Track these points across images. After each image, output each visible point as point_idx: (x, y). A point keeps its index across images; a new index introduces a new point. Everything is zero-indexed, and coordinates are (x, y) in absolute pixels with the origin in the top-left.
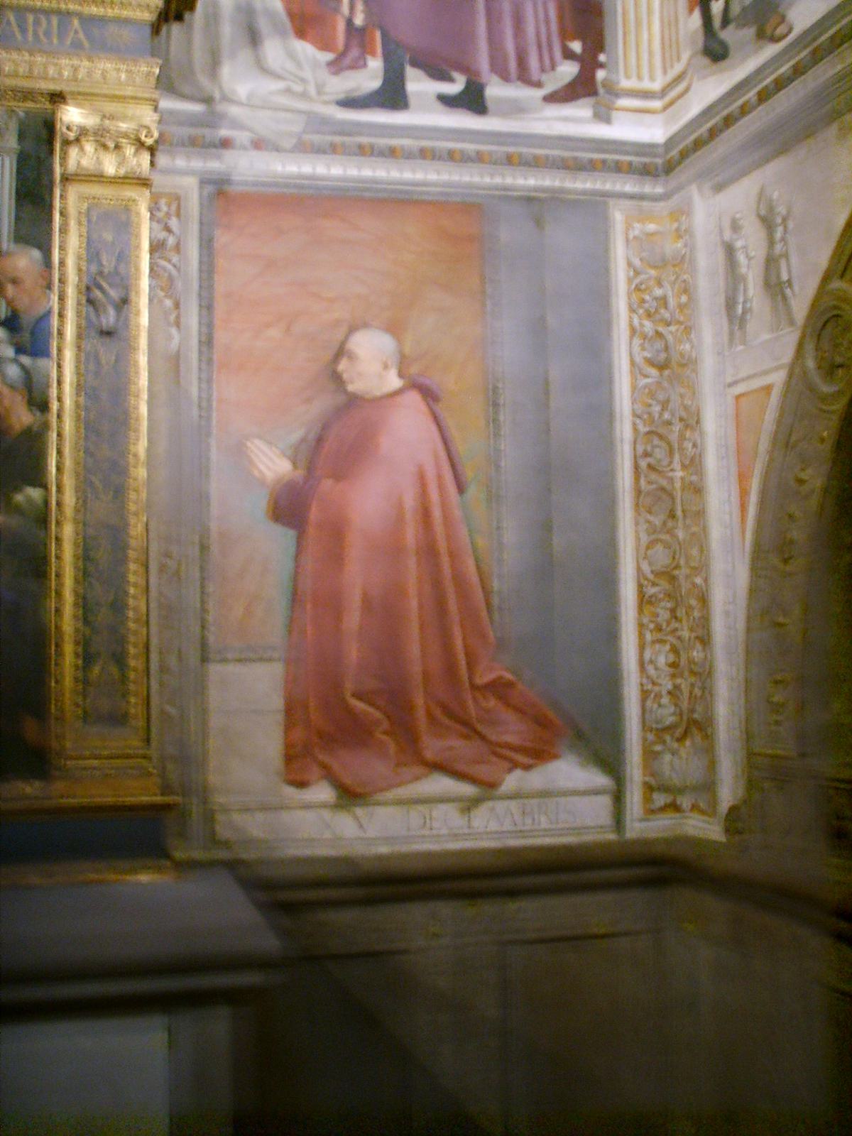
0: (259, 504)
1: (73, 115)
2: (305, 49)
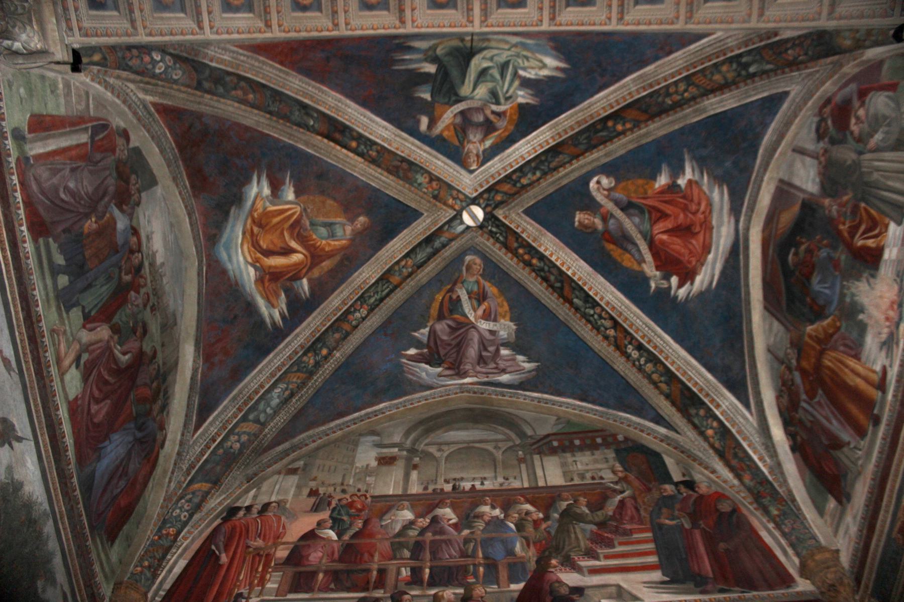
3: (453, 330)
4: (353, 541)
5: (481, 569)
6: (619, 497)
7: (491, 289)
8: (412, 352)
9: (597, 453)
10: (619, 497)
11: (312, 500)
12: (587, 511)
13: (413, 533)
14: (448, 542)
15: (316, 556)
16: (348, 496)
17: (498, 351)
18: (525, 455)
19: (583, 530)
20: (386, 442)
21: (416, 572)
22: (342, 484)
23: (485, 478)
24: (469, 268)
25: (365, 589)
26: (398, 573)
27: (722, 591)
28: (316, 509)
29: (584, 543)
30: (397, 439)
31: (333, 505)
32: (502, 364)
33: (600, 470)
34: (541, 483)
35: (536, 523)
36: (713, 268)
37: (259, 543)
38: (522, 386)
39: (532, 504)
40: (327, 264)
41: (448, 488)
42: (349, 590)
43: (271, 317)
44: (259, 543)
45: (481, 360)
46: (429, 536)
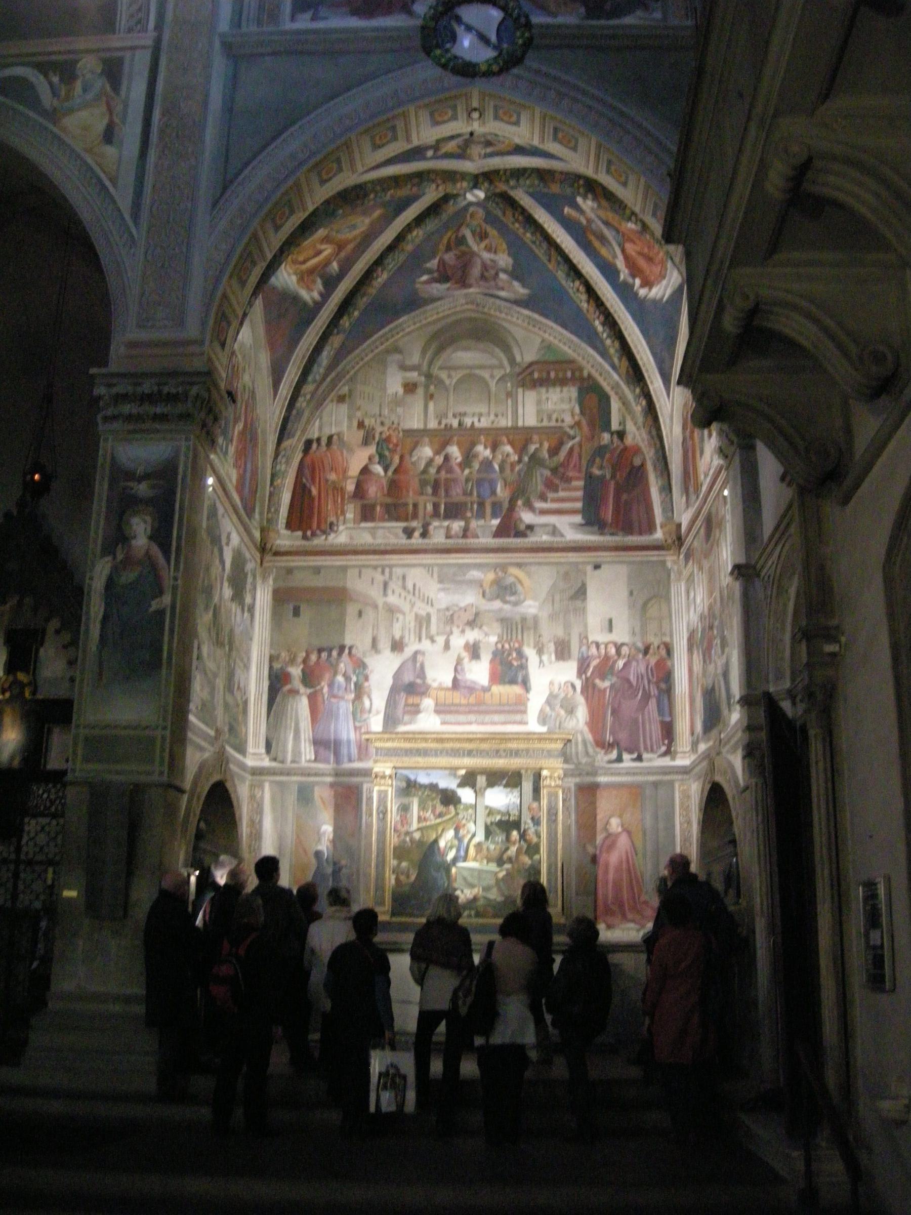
1: (545, 773)
2: (598, 750)
3: (458, 257)
4: (396, 477)
5: (475, 506)
6: (570, 444)
7: (493, 232)
8: (425, 278)
9: (565, 389)
12: (547, 456)
13: (433, 471)
14: (455, 480)
15: (373, 491)
16: (386, 429)
17: (497, 274)
18: (512, 387)
19: (542, 475)
20: (408, 363)
21: (436, 506)
22: (380, 415)
23: (480, 415)
24: (472, 216)
25: (406, 520)
26: (425, 508)
27: (612, 534)
28: (366, 442)
29: (540, 487)
30: (415, 359)
31: (377, 439)
32: (500, 284)
33: (564, 411)
34: (520, 424)
35: (513, 465)
36: (665, 290)
38: (517, 302)
39: (513, 447)
40: (350, 247)
41: (455, 423)
42: (398, 519)
43: (312, 298)
44: (332, 477)
45: (483, 277)
46: (443, 473)
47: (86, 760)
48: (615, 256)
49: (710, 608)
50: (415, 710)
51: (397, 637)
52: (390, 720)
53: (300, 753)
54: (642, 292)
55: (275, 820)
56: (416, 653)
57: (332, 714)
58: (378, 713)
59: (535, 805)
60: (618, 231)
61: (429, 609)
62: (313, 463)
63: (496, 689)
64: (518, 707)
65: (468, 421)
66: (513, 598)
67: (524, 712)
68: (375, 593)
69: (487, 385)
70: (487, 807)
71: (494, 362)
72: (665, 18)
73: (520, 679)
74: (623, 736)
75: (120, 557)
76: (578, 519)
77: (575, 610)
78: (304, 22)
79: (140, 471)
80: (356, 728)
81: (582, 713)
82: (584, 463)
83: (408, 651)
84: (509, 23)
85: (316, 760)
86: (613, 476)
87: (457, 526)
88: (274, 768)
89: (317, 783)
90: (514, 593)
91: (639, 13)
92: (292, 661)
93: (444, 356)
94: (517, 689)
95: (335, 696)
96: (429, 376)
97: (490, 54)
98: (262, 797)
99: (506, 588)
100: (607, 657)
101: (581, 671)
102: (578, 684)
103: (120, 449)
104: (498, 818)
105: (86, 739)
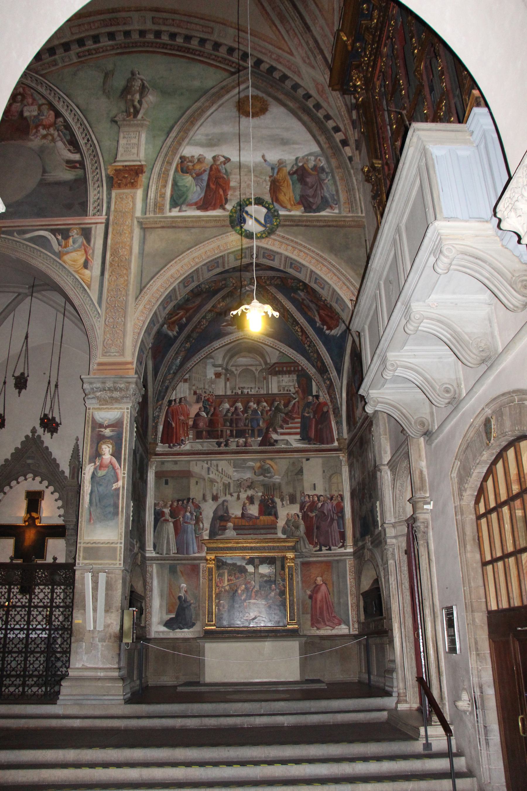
0: (307, 597)
4: (212, 418)
6: (294, 402)
8: (225, 324)
9: (291, 376)
10: (294, 402)
11: (195, 397)
13: (230, 415)
14: (240, 419)
15: (201, 424)
20: (217, 363)
21: (231, 431)
23: (251, 388)
25: (218, 438)
27: (314, 444)
28: (198, 401)
29: (280, 422)
30: (220, 362)
34: (270, 392)
35: (267, 412)
37: (182, 418)
39: (267, 403)
42: (213, 439)
44: (182, 418)
47: (85, 558)
48: (315, 316)
49: (363, 479)
50: (224, 529)
51: (215, 494)
52: (213, 534)
53: (170, 550)
54: (327, 332)
55: (159, 582)
56: (224, 501)
57: (185, 531)
58: (206, 530)
59: (282, 572)
60: (317, 305)
61: (229, 480)
62: (173, 411)
63: (261, 518)
64: (272, 527)
65: (246, 391)
66: (269, 475)
67: (276, 528)
68: (204, 473)
69: (254, 373)
70: (260, 574)
71: (258, 363)
72: (340, 213)
73: (273, 513)
74: (322, 539)
75: (98, 464)
76: (298, 437)
77: (298, 480)
78: (175, 212)
79: (106, 423)
80: (196, 537)
81: (302, 528)
82: (300, 411)
83: (220, 501)
84: (270, 214)
85: (177, 553)
86: (314, 417)
87: (242, 441)
88: (157, 557)
89: (179, 564)
90: (269, 473)
91: (328, 210)
92: (165, 506)
93: (234, 359)
94: (272, 518)
95: (186, 523)
96: (226, 370)
97: (261, 229)
98: (152, 571)
99: (265, 470)
100: (313, 502)
101: (302, 509)
102: (300, 515)
103: (96, 413)
104: (265, 578)
105: (85, 548)
